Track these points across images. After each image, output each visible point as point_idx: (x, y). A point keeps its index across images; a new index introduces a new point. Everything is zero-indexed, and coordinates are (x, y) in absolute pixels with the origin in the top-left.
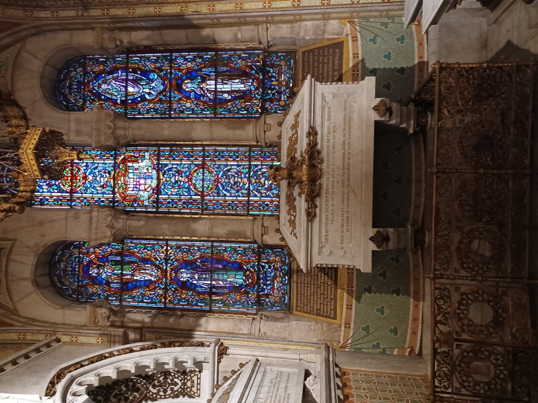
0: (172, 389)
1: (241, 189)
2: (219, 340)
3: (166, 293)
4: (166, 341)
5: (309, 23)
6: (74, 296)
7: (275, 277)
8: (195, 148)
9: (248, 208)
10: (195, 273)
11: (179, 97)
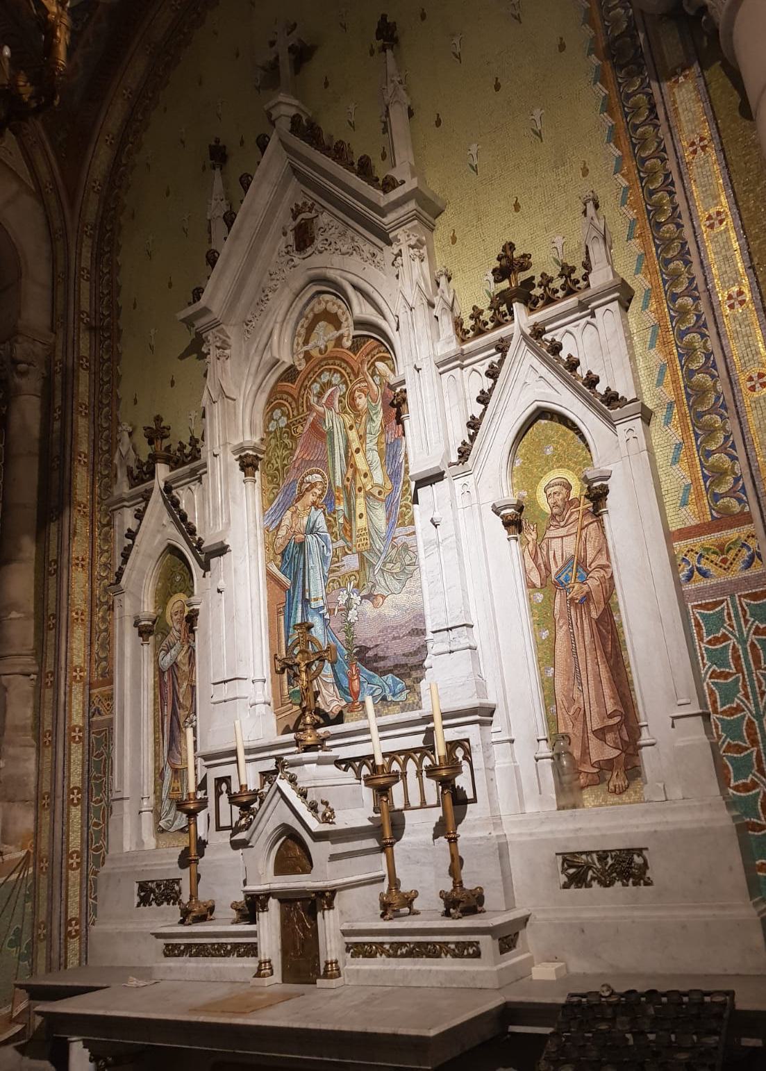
5: (31, 766)
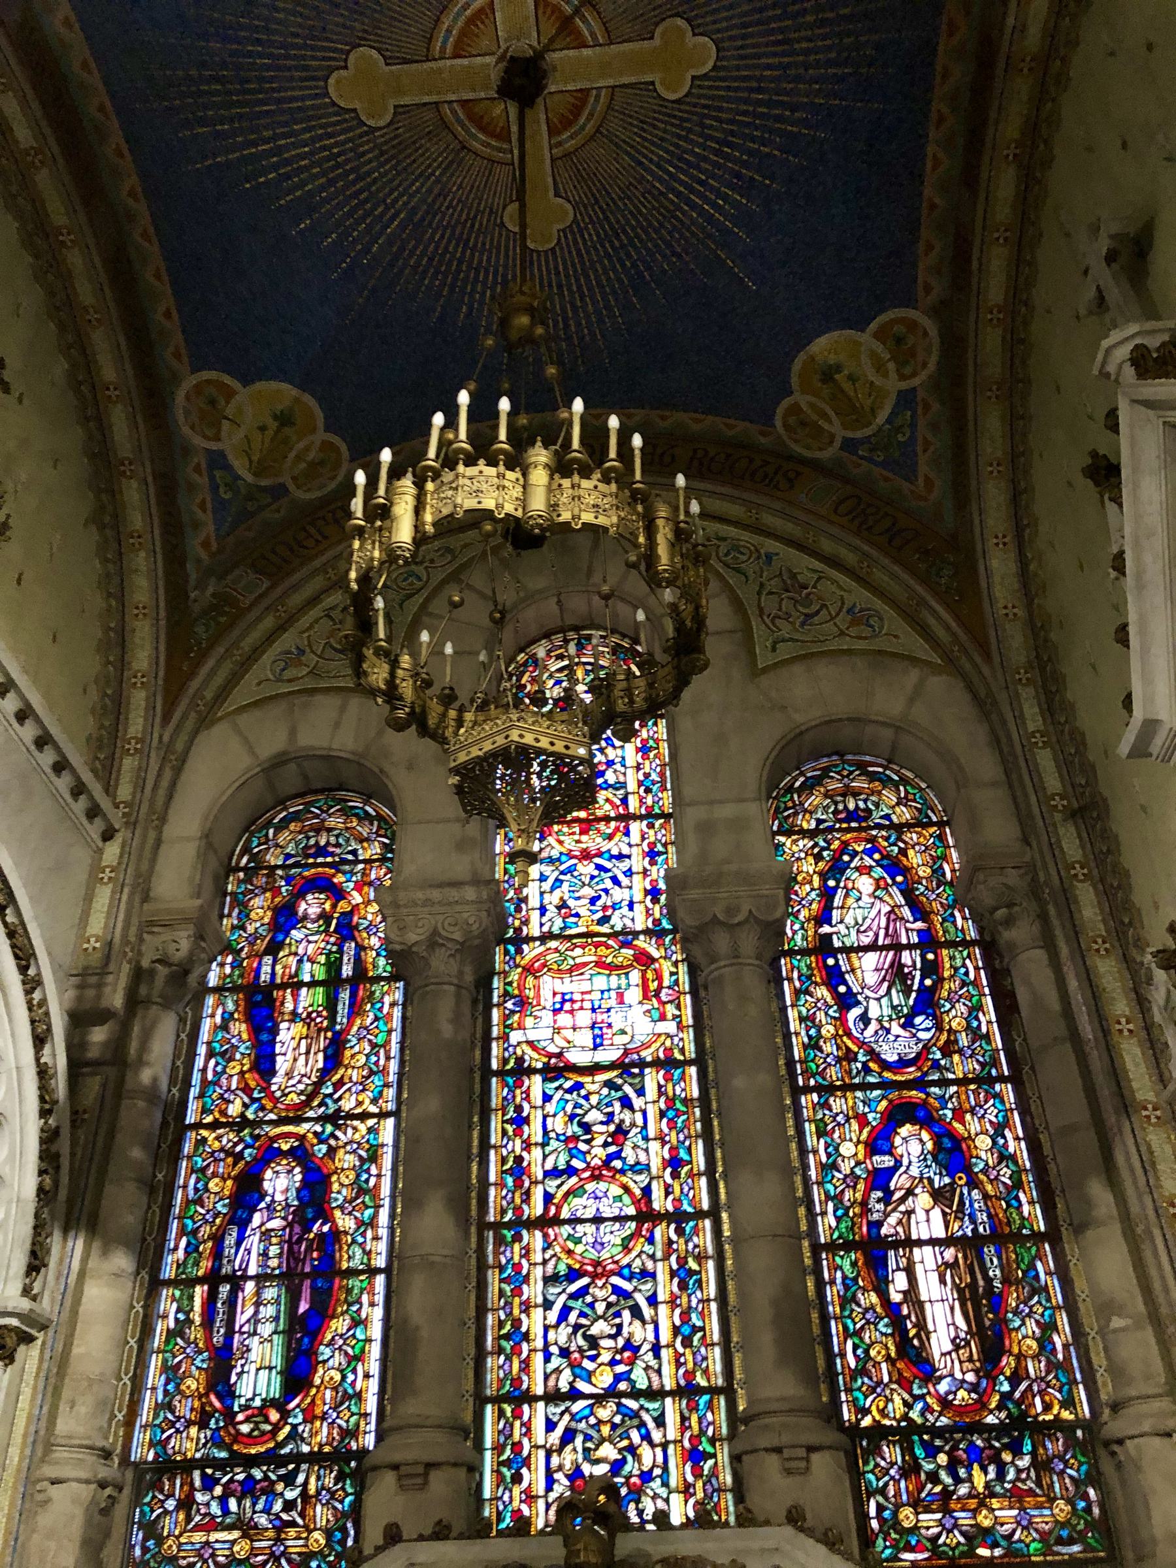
1: (573, 1365)
2: (43, 1327)
3: (230, 1125)
4: (64, 1145)
6: (245, 860)
7: (248, 1529)
8: (703, 1181)
9: (507, 1398)
11: (870, 1116)
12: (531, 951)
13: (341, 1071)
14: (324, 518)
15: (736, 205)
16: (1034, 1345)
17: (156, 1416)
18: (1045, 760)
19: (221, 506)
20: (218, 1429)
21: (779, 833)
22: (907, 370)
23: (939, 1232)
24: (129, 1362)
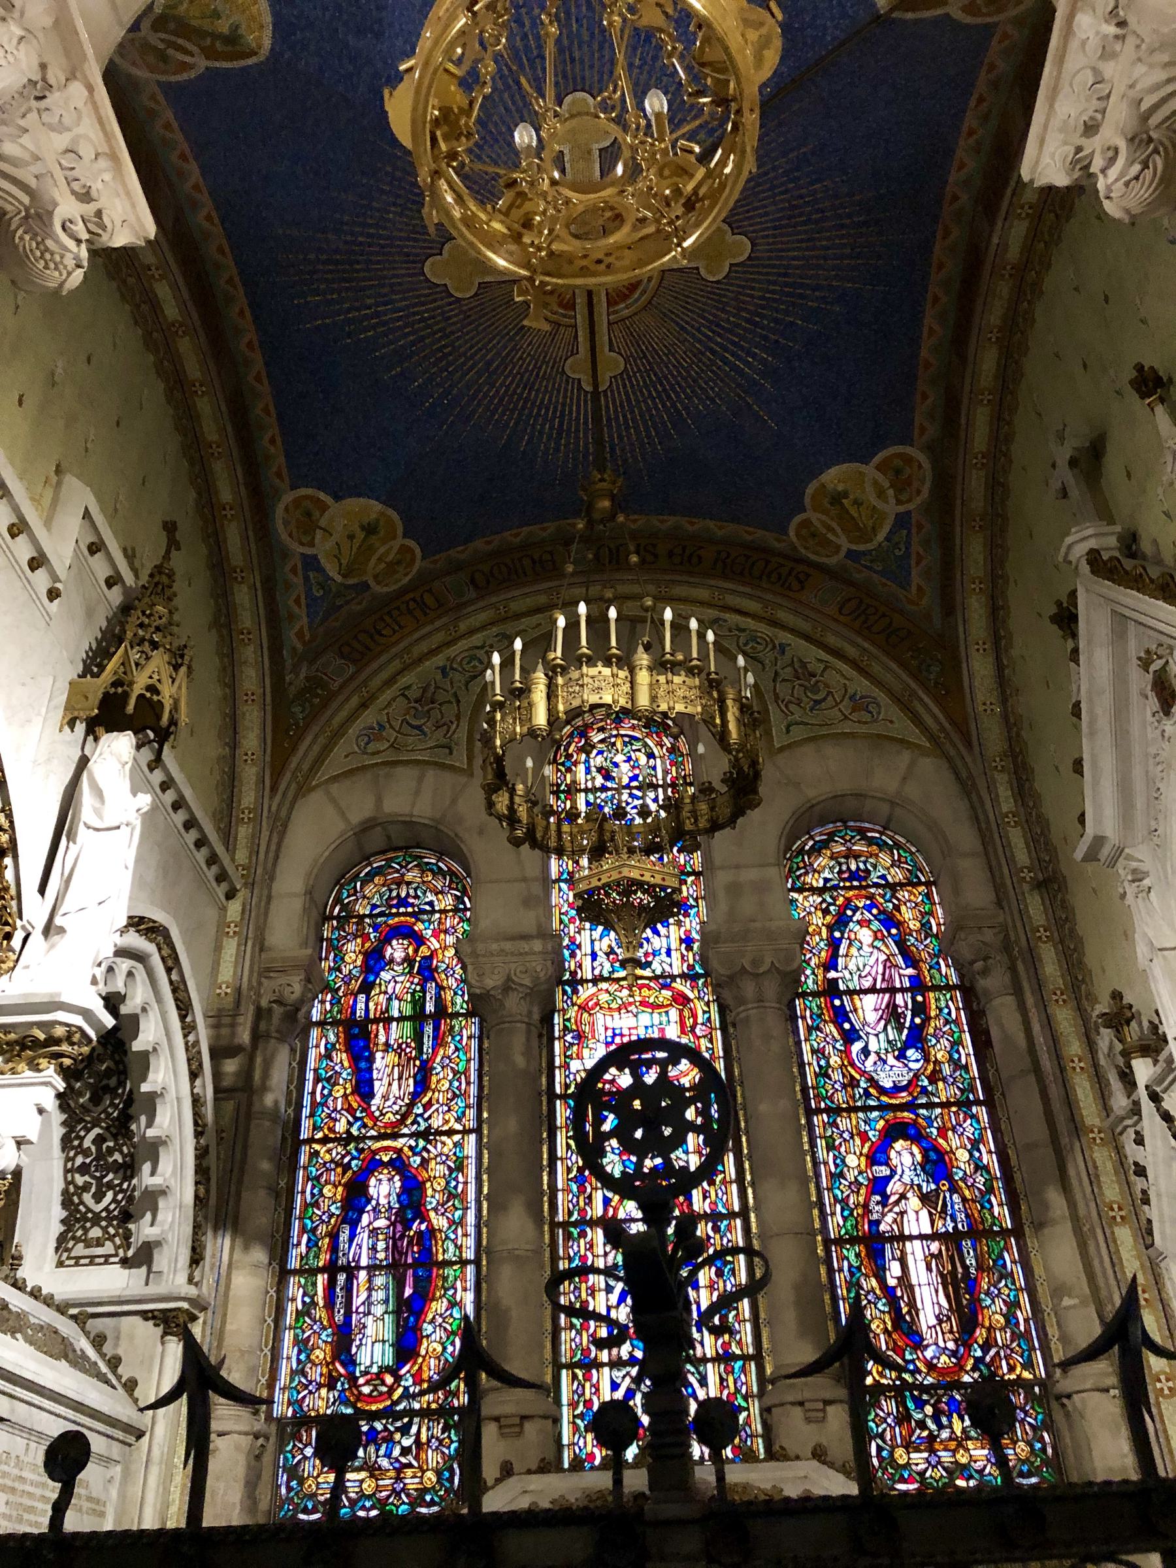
0: (86, 1188)
2: (204, 1309)
4: (212, 1160)
8: (734, 1187)
9: (579, 1365)
10: (389, 1219)
11: (871, 1134)
12: (586, 992)
13: (429, 1094)
14: (398, 608)
15: (763, 362)
16: (1002, 1320)
17: (292, 1380)
18: (1017, 837)
19: (312, 601)
20: (344, 1390)
21: (793, 889)
22: (904, 497)
23: (927, 1230)
24: (267, 1336)
